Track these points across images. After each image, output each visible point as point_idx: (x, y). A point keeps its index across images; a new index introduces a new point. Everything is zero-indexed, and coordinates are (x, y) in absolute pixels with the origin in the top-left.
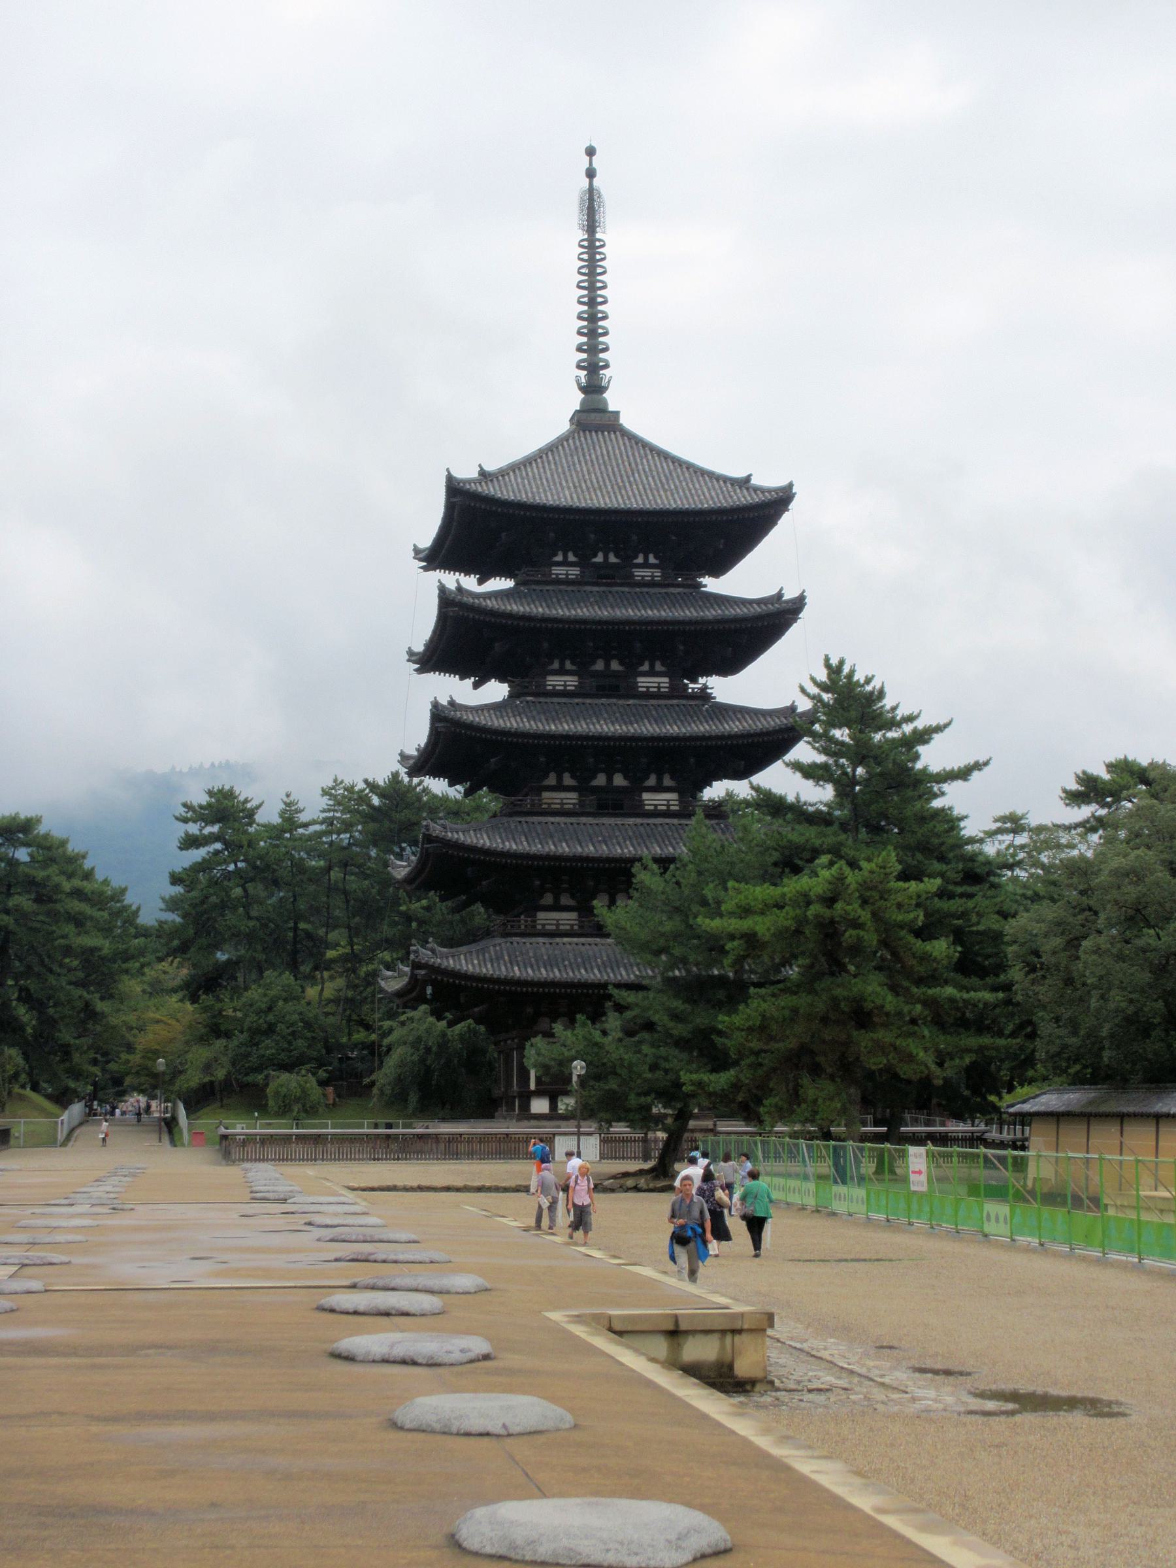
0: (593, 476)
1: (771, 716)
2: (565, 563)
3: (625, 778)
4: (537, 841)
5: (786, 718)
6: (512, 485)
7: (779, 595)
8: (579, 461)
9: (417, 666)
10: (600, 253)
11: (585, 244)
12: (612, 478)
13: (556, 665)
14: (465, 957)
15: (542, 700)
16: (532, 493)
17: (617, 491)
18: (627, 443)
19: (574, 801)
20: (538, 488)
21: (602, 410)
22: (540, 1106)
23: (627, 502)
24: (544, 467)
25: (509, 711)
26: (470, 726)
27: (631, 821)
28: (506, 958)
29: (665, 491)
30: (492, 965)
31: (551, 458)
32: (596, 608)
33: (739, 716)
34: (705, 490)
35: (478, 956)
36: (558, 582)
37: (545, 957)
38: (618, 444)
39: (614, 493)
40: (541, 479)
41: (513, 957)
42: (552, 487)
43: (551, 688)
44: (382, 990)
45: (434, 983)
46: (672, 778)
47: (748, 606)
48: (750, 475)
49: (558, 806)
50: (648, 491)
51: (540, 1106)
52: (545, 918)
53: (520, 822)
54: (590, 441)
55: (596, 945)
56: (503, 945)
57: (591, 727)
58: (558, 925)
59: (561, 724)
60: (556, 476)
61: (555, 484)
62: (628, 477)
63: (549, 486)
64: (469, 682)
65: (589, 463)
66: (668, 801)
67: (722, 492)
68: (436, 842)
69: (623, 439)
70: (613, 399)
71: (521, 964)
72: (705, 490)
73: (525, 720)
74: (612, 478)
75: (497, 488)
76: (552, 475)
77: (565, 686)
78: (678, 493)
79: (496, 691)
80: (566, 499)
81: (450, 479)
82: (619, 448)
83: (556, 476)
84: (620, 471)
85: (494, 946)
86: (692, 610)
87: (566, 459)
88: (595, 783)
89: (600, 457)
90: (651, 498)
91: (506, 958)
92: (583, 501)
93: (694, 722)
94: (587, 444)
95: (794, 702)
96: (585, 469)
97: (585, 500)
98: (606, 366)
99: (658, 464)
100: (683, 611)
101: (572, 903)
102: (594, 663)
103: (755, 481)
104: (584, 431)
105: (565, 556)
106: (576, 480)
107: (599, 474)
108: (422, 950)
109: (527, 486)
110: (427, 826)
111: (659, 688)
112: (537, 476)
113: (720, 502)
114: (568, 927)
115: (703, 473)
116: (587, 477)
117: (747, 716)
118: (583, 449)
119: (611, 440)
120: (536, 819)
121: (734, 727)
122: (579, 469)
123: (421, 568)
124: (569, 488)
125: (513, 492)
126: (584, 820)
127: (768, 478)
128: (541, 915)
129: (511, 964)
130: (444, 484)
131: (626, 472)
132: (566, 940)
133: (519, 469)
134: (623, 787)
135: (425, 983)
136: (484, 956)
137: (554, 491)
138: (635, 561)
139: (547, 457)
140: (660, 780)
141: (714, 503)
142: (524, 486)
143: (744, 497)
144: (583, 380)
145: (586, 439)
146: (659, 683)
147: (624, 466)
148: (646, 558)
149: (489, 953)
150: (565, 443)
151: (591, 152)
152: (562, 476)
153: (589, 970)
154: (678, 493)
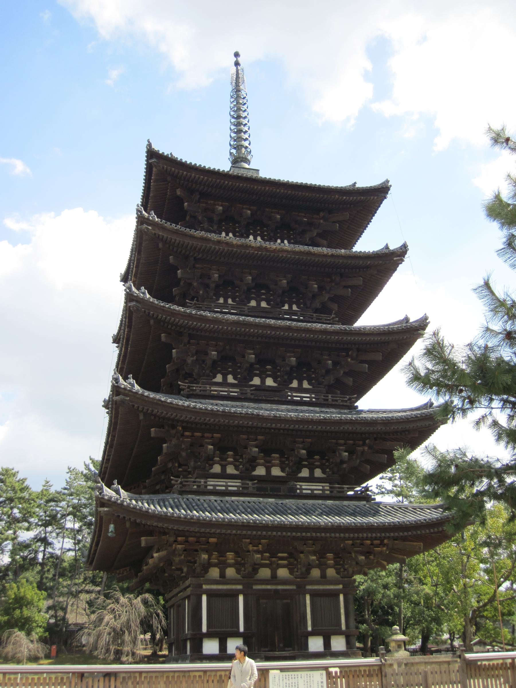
3: (275, 381)
7: (387, 247)
13: (221, 301)
27: (284, 407)
37: (219, 508)
45: (119, 522)
46: (309, 384)
48: (355, 183)
55: (259, 502)
56: (180, 499)
58: (227, 486)
68: (126, 395)
81: (150, 145)
91: (184, 506)
102: (249, 302)
103: (357, 186)
108: (105, 488)
114: (235, 489)
130: (146, 150)
132: (233, 498)
140: (300, 383)
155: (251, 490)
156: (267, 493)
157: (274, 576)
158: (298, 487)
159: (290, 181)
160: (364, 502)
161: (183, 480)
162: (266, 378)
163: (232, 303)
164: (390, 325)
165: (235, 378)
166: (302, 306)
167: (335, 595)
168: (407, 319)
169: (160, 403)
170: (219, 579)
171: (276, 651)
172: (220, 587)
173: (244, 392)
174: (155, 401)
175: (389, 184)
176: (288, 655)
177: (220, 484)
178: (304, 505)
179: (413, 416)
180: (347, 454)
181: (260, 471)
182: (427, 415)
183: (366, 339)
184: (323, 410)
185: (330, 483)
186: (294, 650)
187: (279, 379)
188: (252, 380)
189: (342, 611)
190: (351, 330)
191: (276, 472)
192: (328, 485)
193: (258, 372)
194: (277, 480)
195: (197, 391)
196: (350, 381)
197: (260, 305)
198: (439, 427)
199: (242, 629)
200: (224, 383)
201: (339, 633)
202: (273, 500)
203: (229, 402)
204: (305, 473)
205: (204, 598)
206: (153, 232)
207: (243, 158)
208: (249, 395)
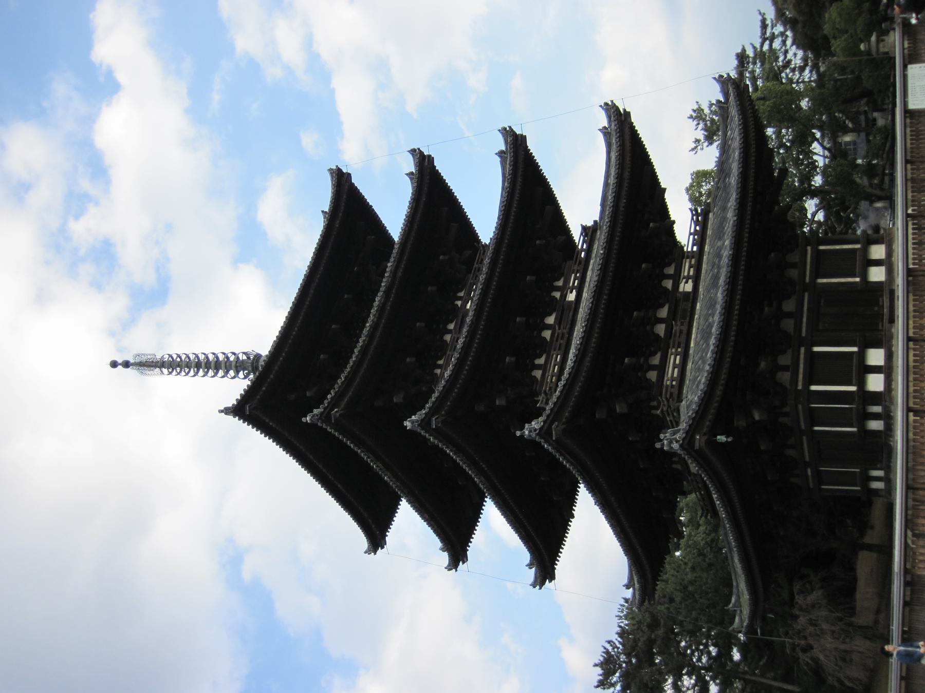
3: (550, 315)
7: (410, 174)
22: (875, 383)
46: (559, 280)
48: (323, 212)
51: (875, 383)
81: (227, 411)
88: (548, 338)
95: (496, 154)
101: (658, 356)
102: (446, 341)
103: (327, 210)
110: (530, 431)
123: (381, 549)
130: (230, 418)
132: (692, 345)
135: (712, 443)
140: (558, 289)
151: (114, 364)
155: (684, 328)
156: (689, 310)
157: (789, 315)
158: (684, 280)
159: (308, 264)
160: (711, 215)
161: (663, 396)
162: (544, 323)
163: (443, 360)
164: (503, 188)
165: (540, 357)
166: (460, 286)
167: (818, 255)
168: (501, 154)
169: (567, 387)
170: (789, 373)
171: (883, 315)
172: (801, 370)
173: (560, 336)
174: (565, 391)
175: (334, 168)
176: (888, 300)
177: (674, 360)
178: (706, 273)
179: (618, 140)
180: (651, 225)
181: (661, 329)
182: (619, 128)
183: (516, 204)
184: (593, 255)
185: (683, 257)
186: (882, 296)
187: (548, 310)
188: (545, 338)
189: (838, 247)
190: (507, 200)
191: (663, 313)
192: (684, 260)
193: (535, 332)
194: (673, 314)
195: (551, 386)
196: (561, 238)
197: (451, 330)
198: (633, 123)
199: (855, 349)
200: (544, 368)
201: (865, 251)
202: (698, 305)
204: (669, 284)
205: (814, 388)
206: (342, 406)
207: (254, 359)
208: (565, 331)
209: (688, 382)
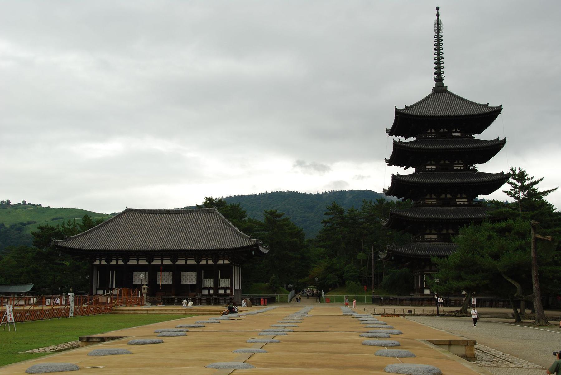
0: (439, 106)
1: (495, 176)
2: (431, 132)
3: (451, 195)
4: (424, 214)
5: (500, 176)
6: (415, 110)
7: (498, 139)
8: (435, 102)
9: (388, 164)
10: (441, 39)
11: (436, 36)
12: (445, 107)
13: (429, 163)
14: (403, 248)
15: (425, 173)
16: (421, 112)
17: (446, 110)
18: (449, 95)
19: (435, 202)
20: (422, 110)
21: (442, 86)
23: (450, 114)
24: (424, 104)
25: (415, 176)
26: (404, 181)
27: (453, 208)
28: (416, 248)
29: (461, 110)
30: (411, 251)
31: (426, 102)
32: (441, 145)
33: (485, 176)
34: (474, 109)
35: (407, 248)
36: (429, 138)
38: (447, 96)
39: (446, 111)
40: (423, 108)
41: (418, 248)
42: (427, 110)
43: (427, 169)
44: (379, 258)
47: (488, 143)
49: (430, 204)
50: (456, 110)
52: (427, 237)
53: (419, 209)
54: (438, 96)
55: (443, 244)
57: (440, 180)
59: (431, 180)
60: (428, 107)
61: (428, 109)
62: (450, 106)
63: (426, 110)
64: (403, 168)
65: (438, 103)
66: (464, 202)
67: (479, 109)
69: (448, 95)
70: (445, 83)
71: (420, 250)
72: (474, 109)
73: (420, 179)
74: (445, 107)
75: (410, 112)
76: (427, 107)
77: (432, 168)
78: (465, 110)
79: (411, 171)
80: (431, 113)
81: (396, 109)
82: (447, 98)
83: (428, 107)
84: (447, 104)
85: (412, 245)
86: (470, 145)
87: (431, 102)
88: (442, 197)
89: (441, 101)
90: (457, 112)
91: (416, 248)
92: (436, 114)
93: (471, 178)
94: (437, 97)
96: (437, 104)
97: (437, 113)
98: (443, 73)
99: (459, 101)
100: (467, 145)
104: (436, 93)
105: (431, 130)
106: (434, 108)
107: (441, 106)
109: (419, 110)
111: (460, 168)
112: (422, 107)
113: (479, 112)
115: (473, 103)
116: (437, 107)
117: (488, 176)
118: (436, 98)
119: (445, 95)
120: (424, 208)
121: (485, 179)
122: (435, 104)
124: (432, 110)
125: (415, 112)
126: (438, 208)
127: (494, 104)
128: (426, 236)
129: (417, 250)
131: (449, 104)
133: (417, 105)
134: (450, 198)
136: (409, 248)
137: (427, 111)
138: (453, 131)
139: (425, 101)
141: (477, 112)
142: (418, 110)
143: (486, 110)
144: (436, 78)
145: (437, 95)
146: (460, 167)
147: (449, 103)
148: (456, 130)
149: (410, 247)
150: (431, 97)
151: (438, 8)
152: (430, 107)
153: (440, 252)
154: (465, 110)
168: (503, 173)
175: (502, 108)
181: (444, 232)
188: (441, 195)
197: (445, 162)
200: (431, 198)
202: (448, 243)
203: (432, 208)
205: (424, 276)
209: (421, 243)
